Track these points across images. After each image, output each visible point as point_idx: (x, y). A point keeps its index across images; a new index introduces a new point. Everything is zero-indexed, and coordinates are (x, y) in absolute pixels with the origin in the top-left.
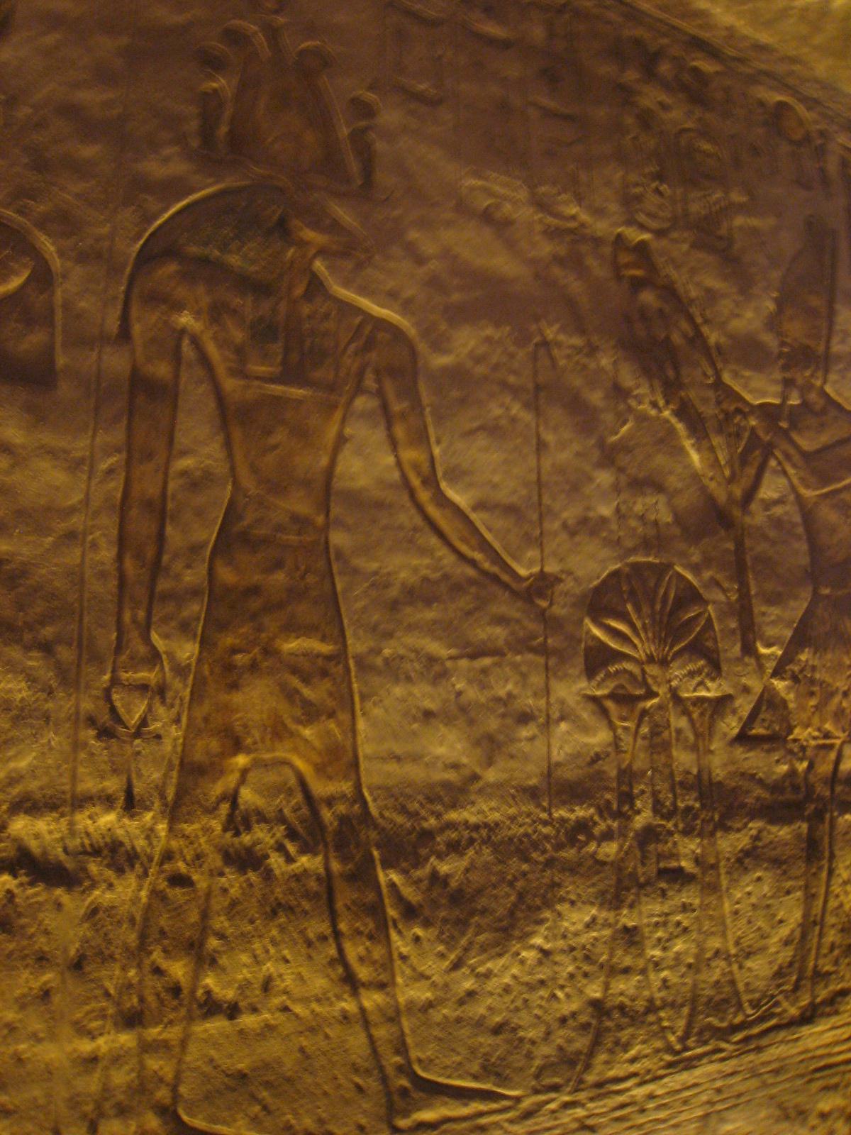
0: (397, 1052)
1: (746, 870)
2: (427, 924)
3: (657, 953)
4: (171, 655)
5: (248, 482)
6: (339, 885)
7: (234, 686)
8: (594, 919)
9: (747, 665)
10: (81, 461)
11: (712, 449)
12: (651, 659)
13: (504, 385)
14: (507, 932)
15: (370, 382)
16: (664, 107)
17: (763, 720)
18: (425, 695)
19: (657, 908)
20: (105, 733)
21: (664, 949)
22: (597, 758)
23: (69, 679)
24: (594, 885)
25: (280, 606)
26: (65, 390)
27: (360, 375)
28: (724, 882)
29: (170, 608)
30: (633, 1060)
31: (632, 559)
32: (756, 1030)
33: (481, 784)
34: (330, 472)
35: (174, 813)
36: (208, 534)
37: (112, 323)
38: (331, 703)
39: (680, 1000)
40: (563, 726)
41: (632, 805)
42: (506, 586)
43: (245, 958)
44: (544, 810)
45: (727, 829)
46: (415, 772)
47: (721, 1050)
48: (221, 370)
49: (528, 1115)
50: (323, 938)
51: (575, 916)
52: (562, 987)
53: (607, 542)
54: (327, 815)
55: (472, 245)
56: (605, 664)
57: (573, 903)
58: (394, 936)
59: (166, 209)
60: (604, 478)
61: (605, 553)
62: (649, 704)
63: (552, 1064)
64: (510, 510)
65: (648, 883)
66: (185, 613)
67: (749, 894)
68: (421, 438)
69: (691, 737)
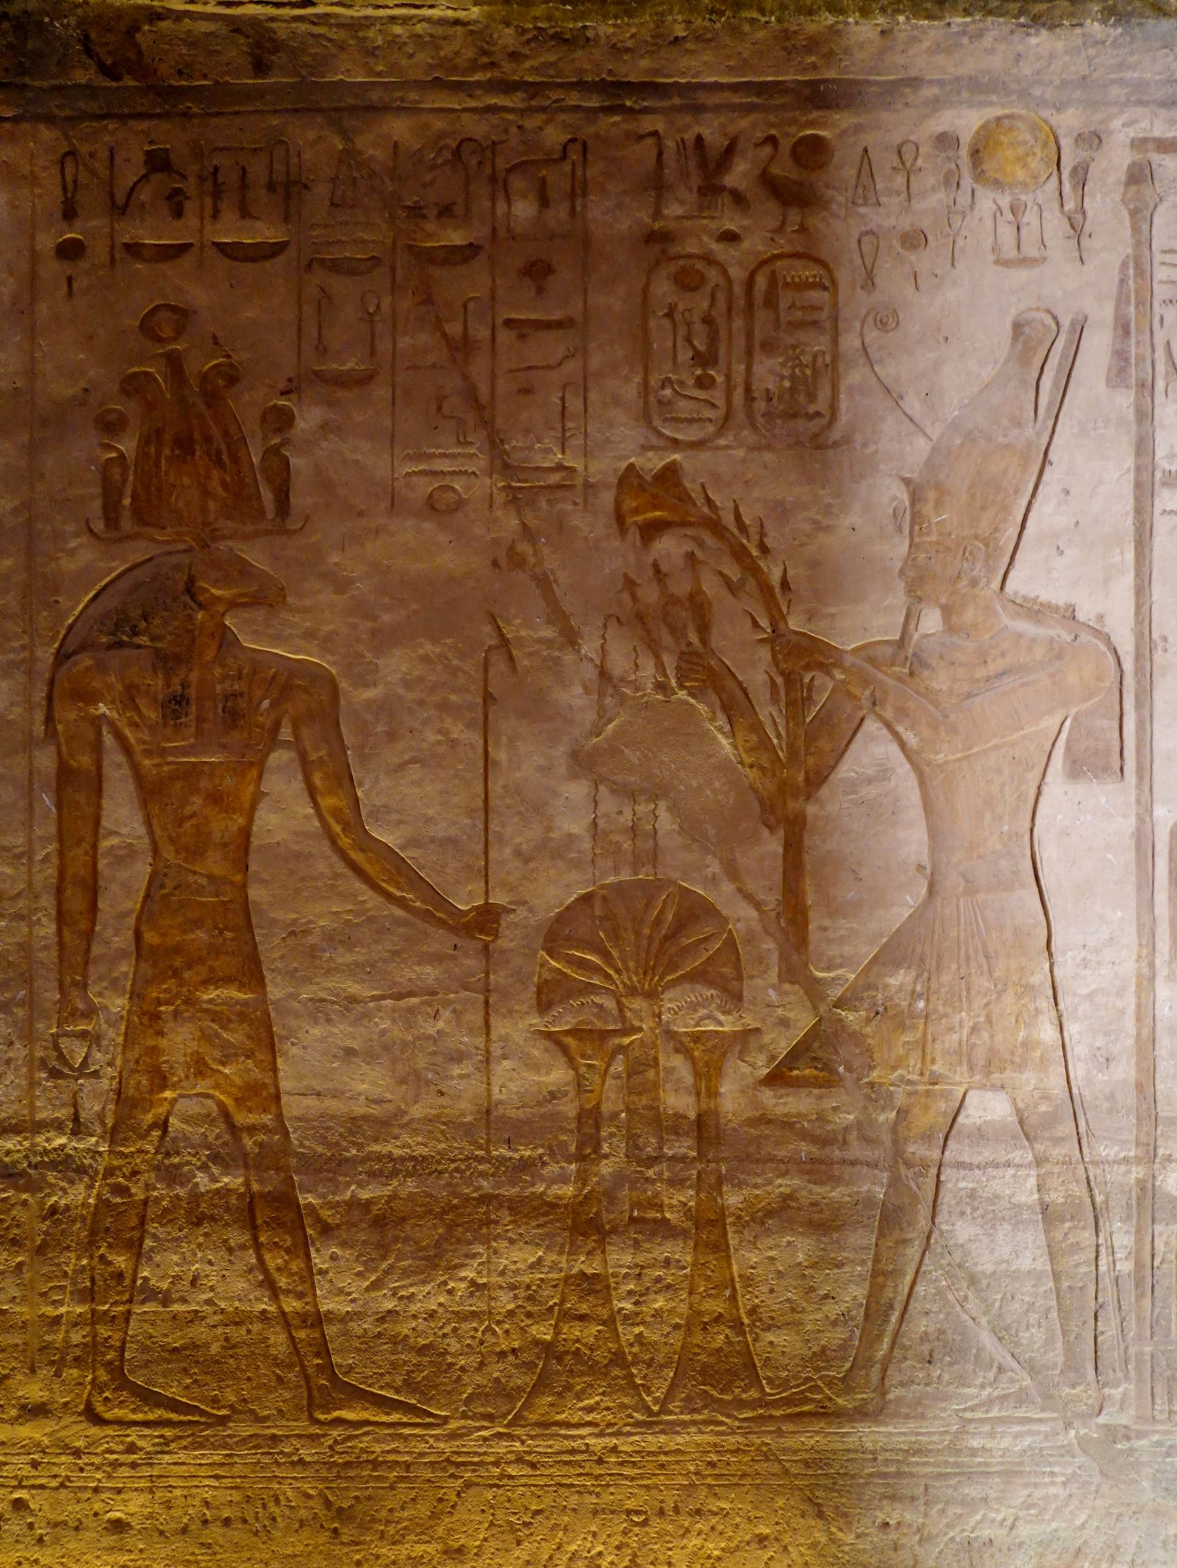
0: (317, 1355)
1: (768, 1232)
2: (344, 1244)
3: (628, 1306)
4: (105, 1008)
5: (168, 852)
6: (259, 1204)
7: (161, 1033)
8: (540, 1260)
9: (787, 993)
10: (21, 855)
11: (757, 727)
12: (632, 991)
13: (445, 707)
14: (434, 1261)
15: (286, 733)
16: (730, 237)
17: (815, 1059)
18: (343, 1033)
19: (628, 1259)
20: (55, 1074)
21: (636, 1303)
22: (553, 1095)
24: (538, 1226)
25: (201, 960)
27: (277, 725)
28: (733, 1241)
29: (102, 969)
30: (590, 1410)
31: (611, 879)
32: (777, 1413)
33: (407, 1118)
34: (246, 833)
35: (113, 1135)
36: (134, 904)
37: (39, 729)
38: (249, 1045)
39: (660, 1358)
40: (506, 1064)
41: (597, 1147)
42: (442, 923)
43: (175, 1258)
44: (480, 1148)
45: (740, 1185)
46: (333, 1105)
47: (722, 1423)
48: (138, 748)
49: (453, 1436)
50: (243, 1247)
51: (516, 1255)
52: (499, 1323)
53: (577, 865)
54: (248, 1142)
55: (414, 548)
56: (570, 995)
57: (512, 1241)
58: (312, 1251)
60: (578, 790)
61: (573, 876)
62: (626, 1041)
63: (487, 1395)
64: (450, 842)
65: (614, 1231)
66: (115, 974)
67: (772, 1259)
68: (344, 780)
69: (689, 1079)
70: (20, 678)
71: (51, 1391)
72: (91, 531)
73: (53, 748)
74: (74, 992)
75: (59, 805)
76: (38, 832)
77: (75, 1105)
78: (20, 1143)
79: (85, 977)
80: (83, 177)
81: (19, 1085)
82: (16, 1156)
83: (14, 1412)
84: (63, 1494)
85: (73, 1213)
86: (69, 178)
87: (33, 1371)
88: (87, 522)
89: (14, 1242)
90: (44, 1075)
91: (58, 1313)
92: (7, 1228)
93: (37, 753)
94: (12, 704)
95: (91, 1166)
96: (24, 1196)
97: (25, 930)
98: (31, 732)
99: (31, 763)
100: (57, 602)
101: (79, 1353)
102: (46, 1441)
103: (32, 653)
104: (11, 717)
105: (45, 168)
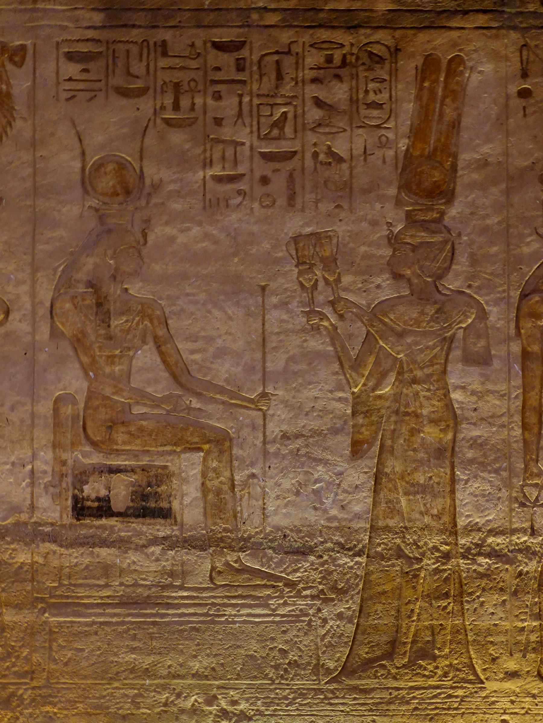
10: (504, 395)
20: (522, 505)
23: (509, 485)
26: (496, 364)
37: (513, 332)
59: (532, 269)
70: (503, 306)
71: (521, 665)
72: (537, 233)
73: (520, 342)
74: (532, 464)
75: (523, 370)
76: (513, 383)
77: (532, 520)
78: (504, 539)
79: (538, 456)
80: (532, 58)
81: (504, 510)
82: (502, 546)
83: (502, 676)
84: (527, 717)
85: (531, 575)
86: (524, 58)
87: (511, 655)
88: (536, 229)
89: (501, 589)
90: (516, 505)
91: (523, 625)
92: (498, 583)
93: (511, 344)
94: (499, 319)
95: (539, 551)
96: (507, 566)
97: (506, 433)
98: (508, 333)
99: (508, 349)
100: (521, 268)
101: (534, 646)
102: (518, 690)
103: (508, 294)
104: (498, 326)
105: (513, 53)
